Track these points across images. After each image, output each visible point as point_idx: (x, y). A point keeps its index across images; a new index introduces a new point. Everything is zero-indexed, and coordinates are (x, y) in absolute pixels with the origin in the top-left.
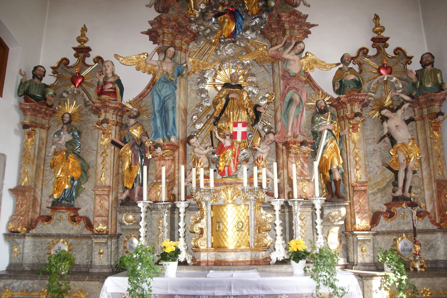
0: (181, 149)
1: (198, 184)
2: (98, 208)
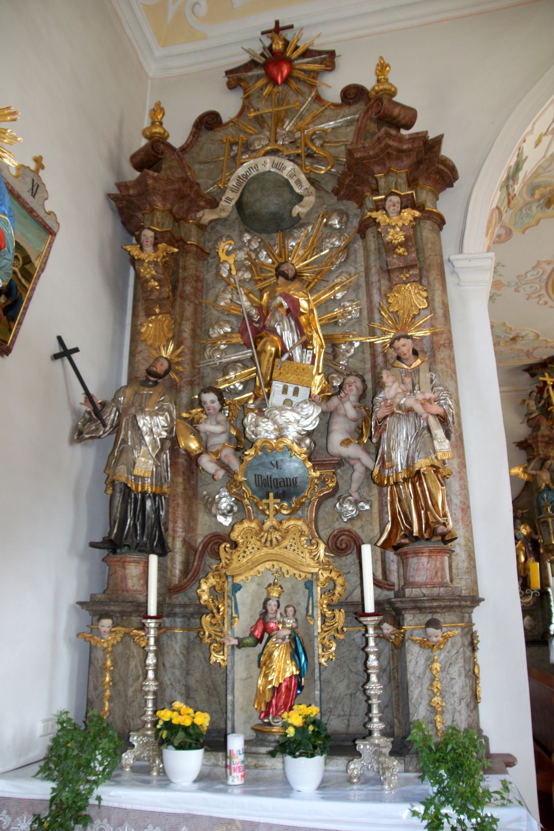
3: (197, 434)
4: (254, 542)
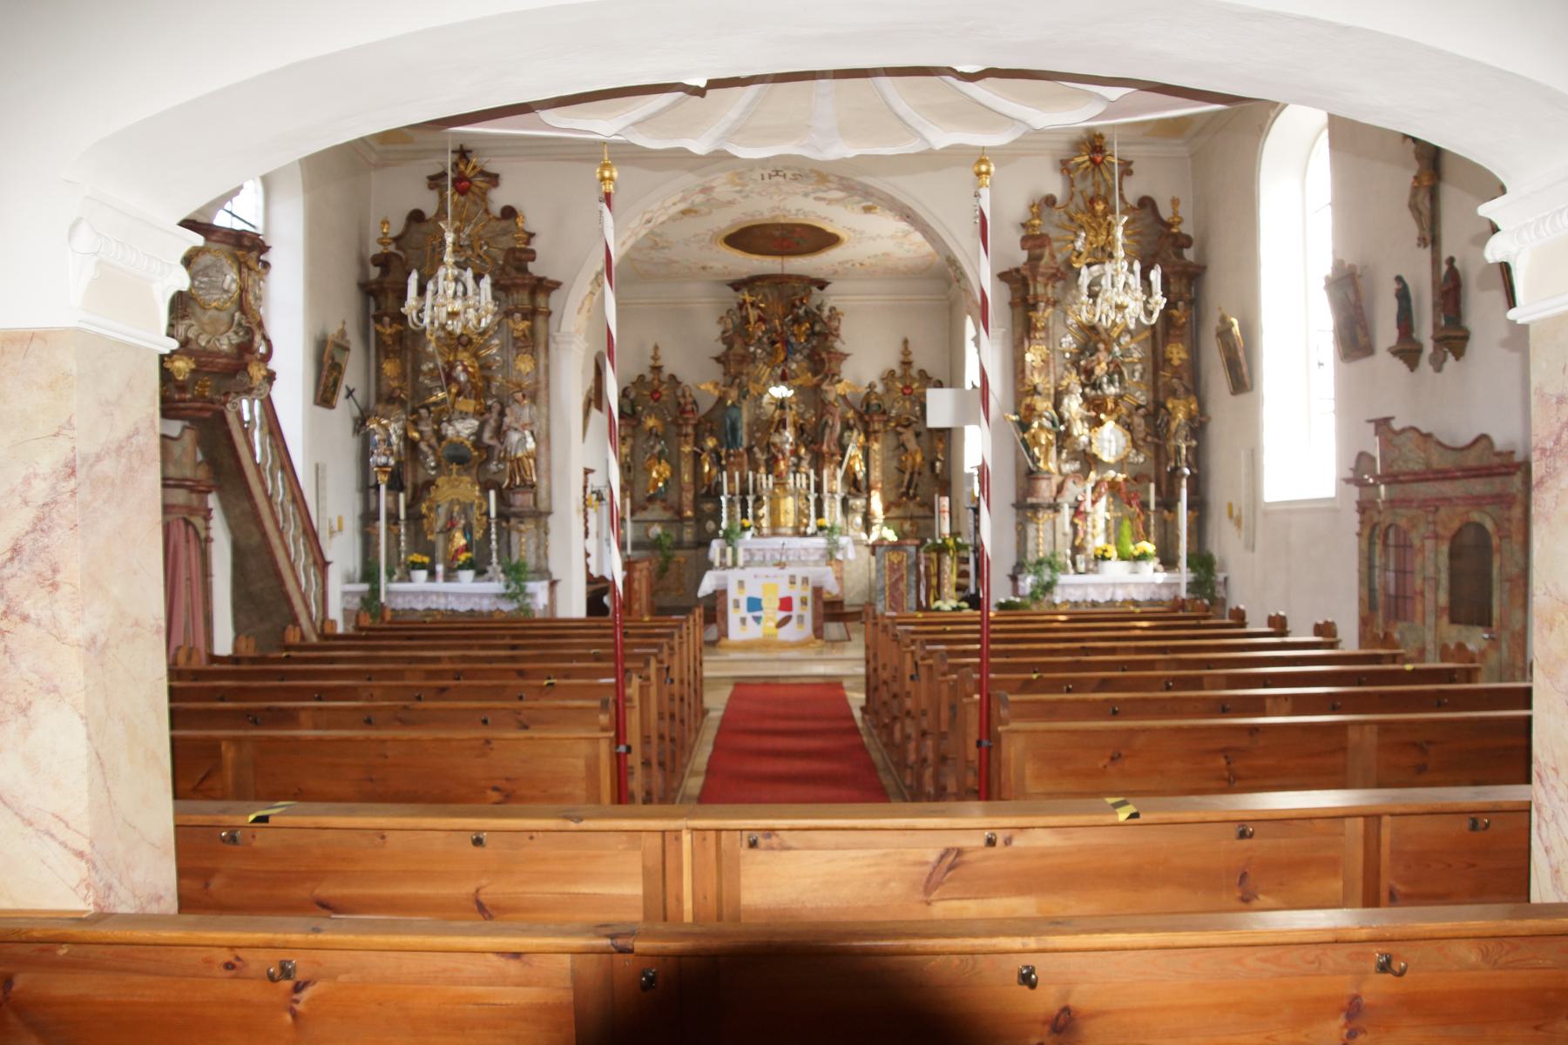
0: (746, 456)
1: (761, 484)
2: (684, 499)
3: (417, 431)
4: (446, 487)
